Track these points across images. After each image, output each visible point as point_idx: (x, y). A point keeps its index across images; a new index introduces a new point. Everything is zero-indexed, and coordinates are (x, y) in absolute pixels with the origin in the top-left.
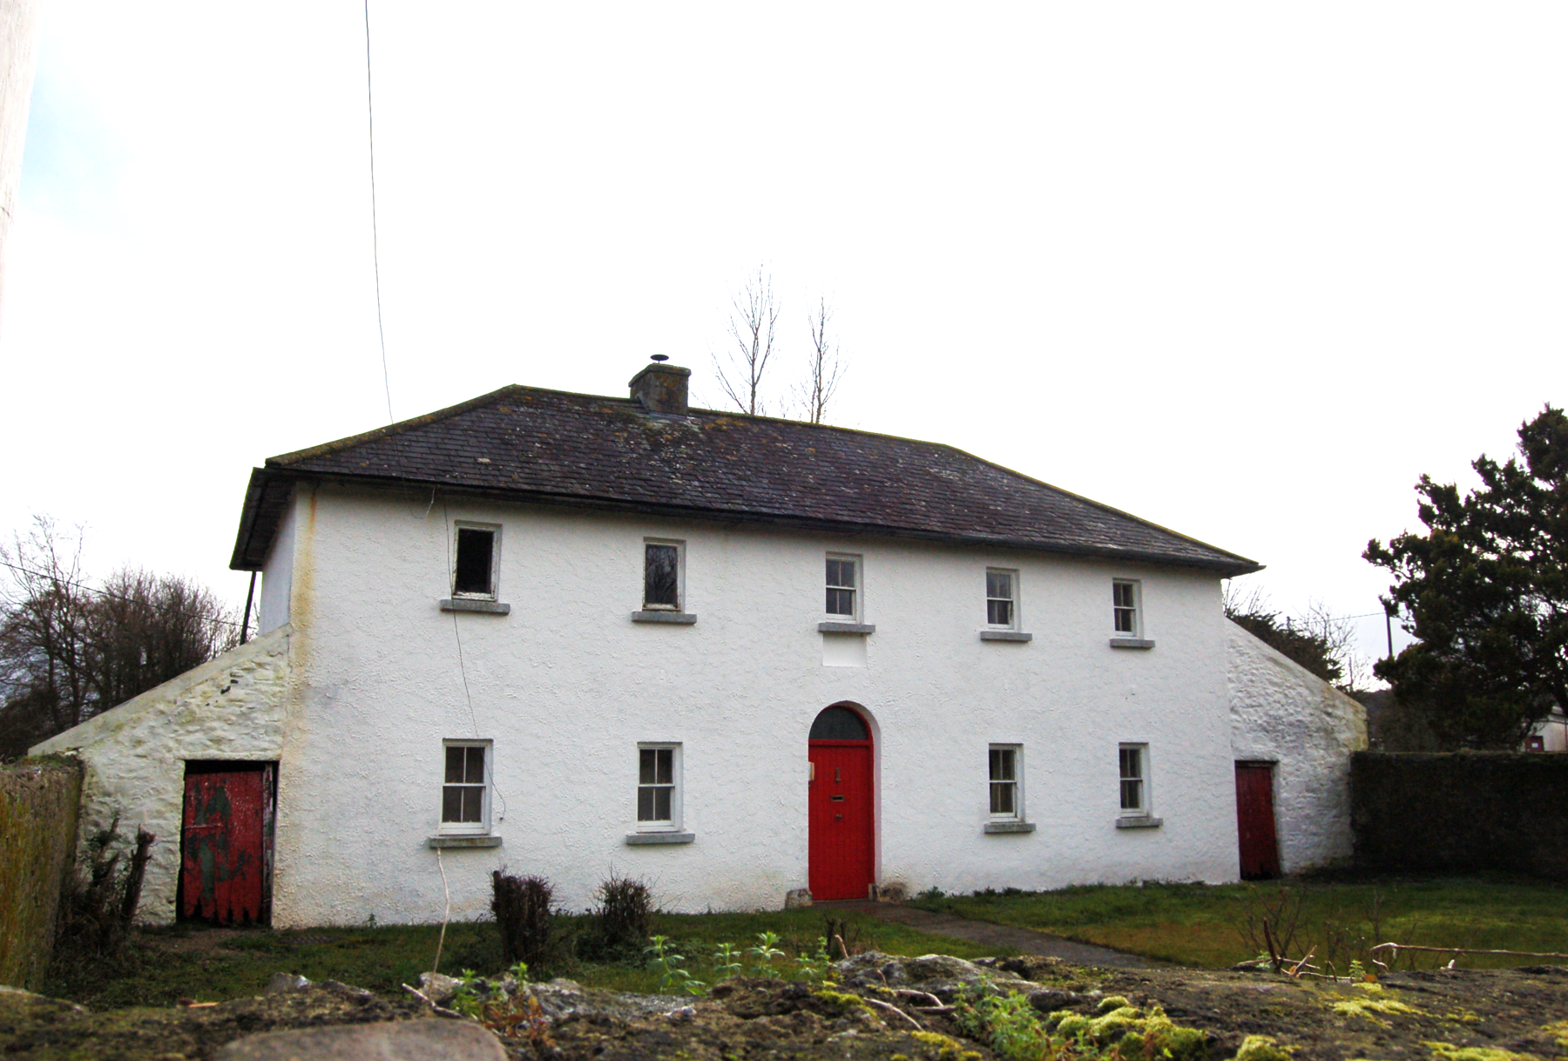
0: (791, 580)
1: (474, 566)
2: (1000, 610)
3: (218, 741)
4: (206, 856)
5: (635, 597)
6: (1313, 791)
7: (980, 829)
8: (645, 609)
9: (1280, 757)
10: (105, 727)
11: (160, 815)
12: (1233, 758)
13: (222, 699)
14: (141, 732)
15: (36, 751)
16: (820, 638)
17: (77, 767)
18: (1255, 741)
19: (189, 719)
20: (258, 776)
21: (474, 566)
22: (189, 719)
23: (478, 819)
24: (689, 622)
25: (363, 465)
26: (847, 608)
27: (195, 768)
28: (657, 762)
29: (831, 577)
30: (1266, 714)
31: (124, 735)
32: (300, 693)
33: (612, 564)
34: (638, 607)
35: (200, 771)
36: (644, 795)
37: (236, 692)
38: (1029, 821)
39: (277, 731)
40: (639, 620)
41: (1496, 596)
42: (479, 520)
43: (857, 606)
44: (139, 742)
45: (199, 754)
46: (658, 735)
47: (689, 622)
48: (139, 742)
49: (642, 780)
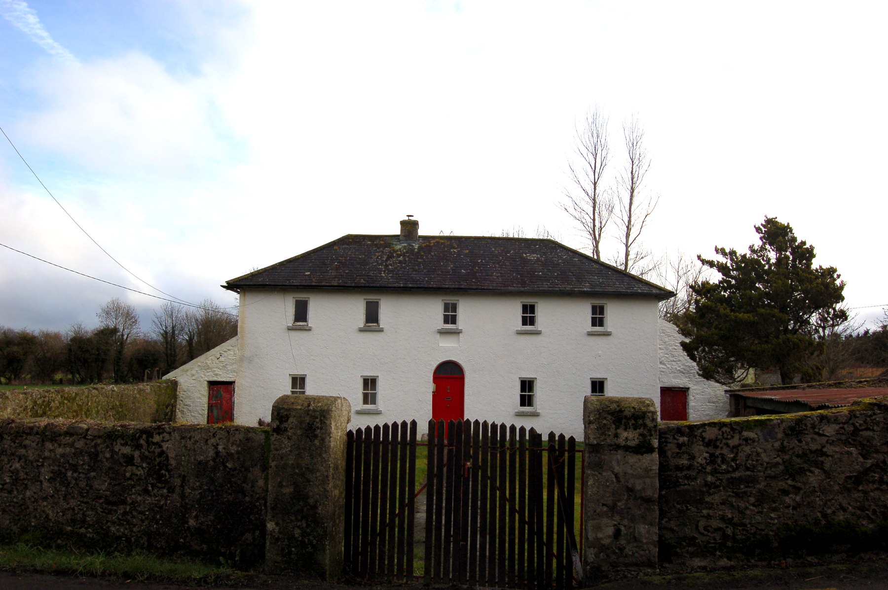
0: (427, 312)
1: (301, 314)
2: (450, 319)
3: (216, 375)
4: (215, 412)
5: (518, 325)
6: (713, 403)
7: (513, 413)
8: (365, 326)
9: (690, 386)
10: (183, 371)
11: (200, 398)
12: (659, 386)
13: (217, 361)
14: (194, 372)
15: (164, 378)
16: (438, 335)
17: (175, 384)
18: (674, 378)
19: (207, 368)
20: (229, 385)
21: (301, 314)
22: (207, 368)
23: (375, 403)
24: (381, 330)
25: (260, 280)
26: (601, 324)
27: (212, 384)
28: (527, 385)
29: (594, 312)
30: (683, 365)
31: (189, 373)
32: (242, 359)
33: (353, 309)
34: (362, 325)
35: (213, 385)
36: (522, 398)
37: (222, 359)
38: (538, 411)
39: (234, 371)
40: (361, 330)
41: (714, 291)
42: (302, 296)
43: (536, 324)
44: (193, 375)
45: (211, 379)
46: (369, 373)
47: (381, 330)
48: (193, 375)
49: (364, 389)
